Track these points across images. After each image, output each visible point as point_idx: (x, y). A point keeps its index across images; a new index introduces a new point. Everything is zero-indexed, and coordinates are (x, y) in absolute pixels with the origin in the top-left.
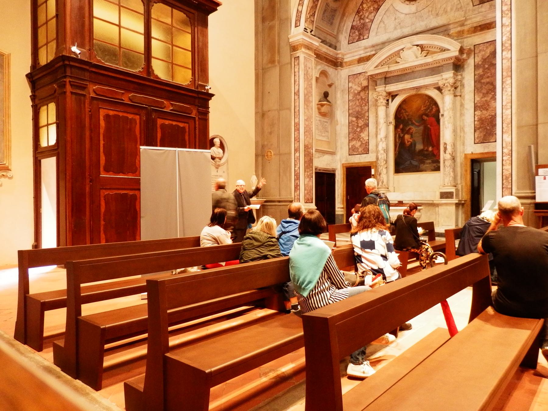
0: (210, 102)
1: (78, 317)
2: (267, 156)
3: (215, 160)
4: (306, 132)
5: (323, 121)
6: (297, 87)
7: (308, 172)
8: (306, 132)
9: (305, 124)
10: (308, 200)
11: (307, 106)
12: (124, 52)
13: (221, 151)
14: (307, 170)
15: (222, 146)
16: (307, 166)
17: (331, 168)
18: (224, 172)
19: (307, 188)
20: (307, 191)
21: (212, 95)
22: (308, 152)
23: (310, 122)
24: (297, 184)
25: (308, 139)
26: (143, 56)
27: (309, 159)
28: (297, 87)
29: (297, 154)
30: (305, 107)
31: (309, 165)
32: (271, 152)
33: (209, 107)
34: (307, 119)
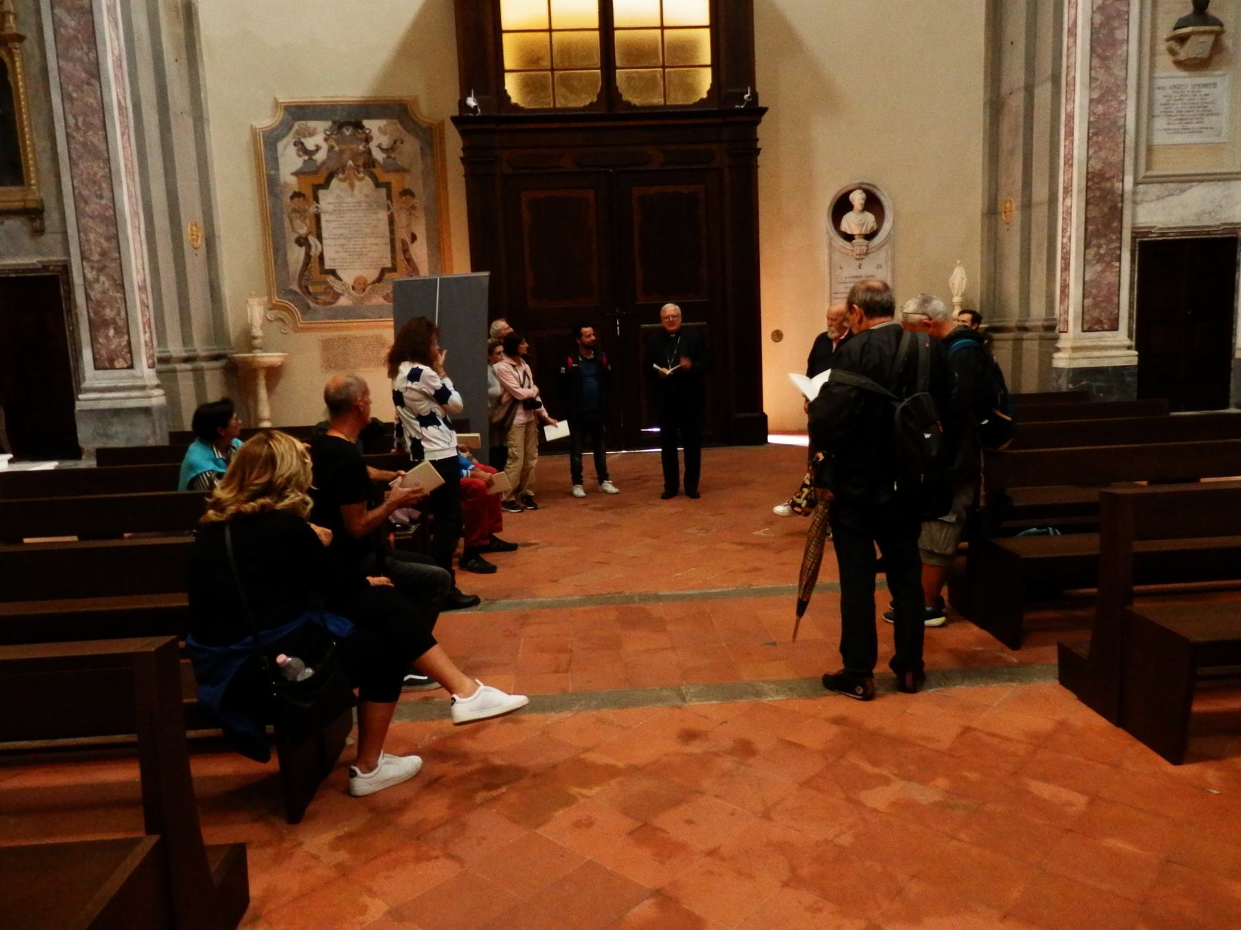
0: (759, 128)
1: (495, 534)
2: (1005, 212)
3: (854, 241)
4: (1096, 134)
5: (1194, 86)
6: (1073, 11)
7: (1100, 246)
8: (1096, 134)
9: (1091, 113)
10: (1100, 322)
11: (1103, 58)
12: (561, 76)
13: (870, 218)
14: (1094, 242)
15: (873, 203)
16: (1098, 230)
17: (1218, 223)
18: (879, 266)
19: (1094, 291)
20: (1094, 299)
21: (765, 110)
22: (1102, 190)
23: (1114, 103)
24: (1065, 280)
25: (1103, 154)
26: (599, 71)
27: (1106, 210)
28: (1073, 11)
29: (1068, 202)
30: (1096, 62)
31: (1107, 226)
32: (1010, 201)
33: (758, 136)
34: (1102, 96)
